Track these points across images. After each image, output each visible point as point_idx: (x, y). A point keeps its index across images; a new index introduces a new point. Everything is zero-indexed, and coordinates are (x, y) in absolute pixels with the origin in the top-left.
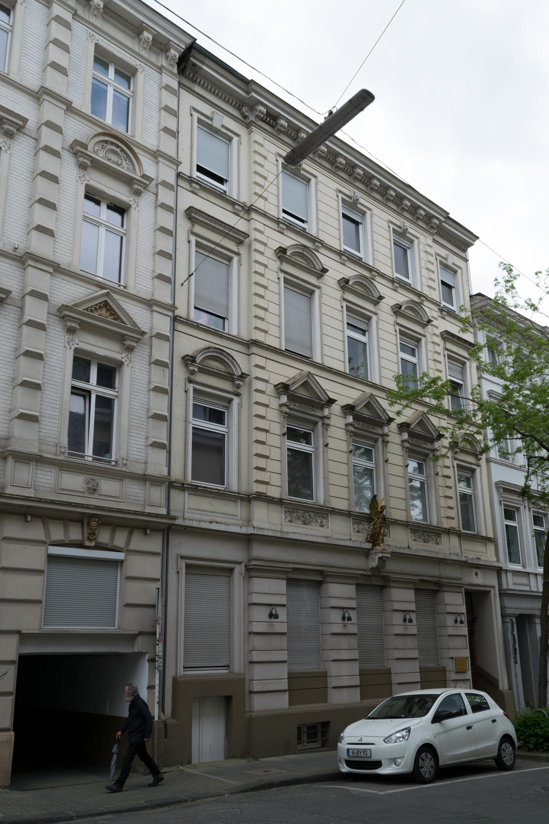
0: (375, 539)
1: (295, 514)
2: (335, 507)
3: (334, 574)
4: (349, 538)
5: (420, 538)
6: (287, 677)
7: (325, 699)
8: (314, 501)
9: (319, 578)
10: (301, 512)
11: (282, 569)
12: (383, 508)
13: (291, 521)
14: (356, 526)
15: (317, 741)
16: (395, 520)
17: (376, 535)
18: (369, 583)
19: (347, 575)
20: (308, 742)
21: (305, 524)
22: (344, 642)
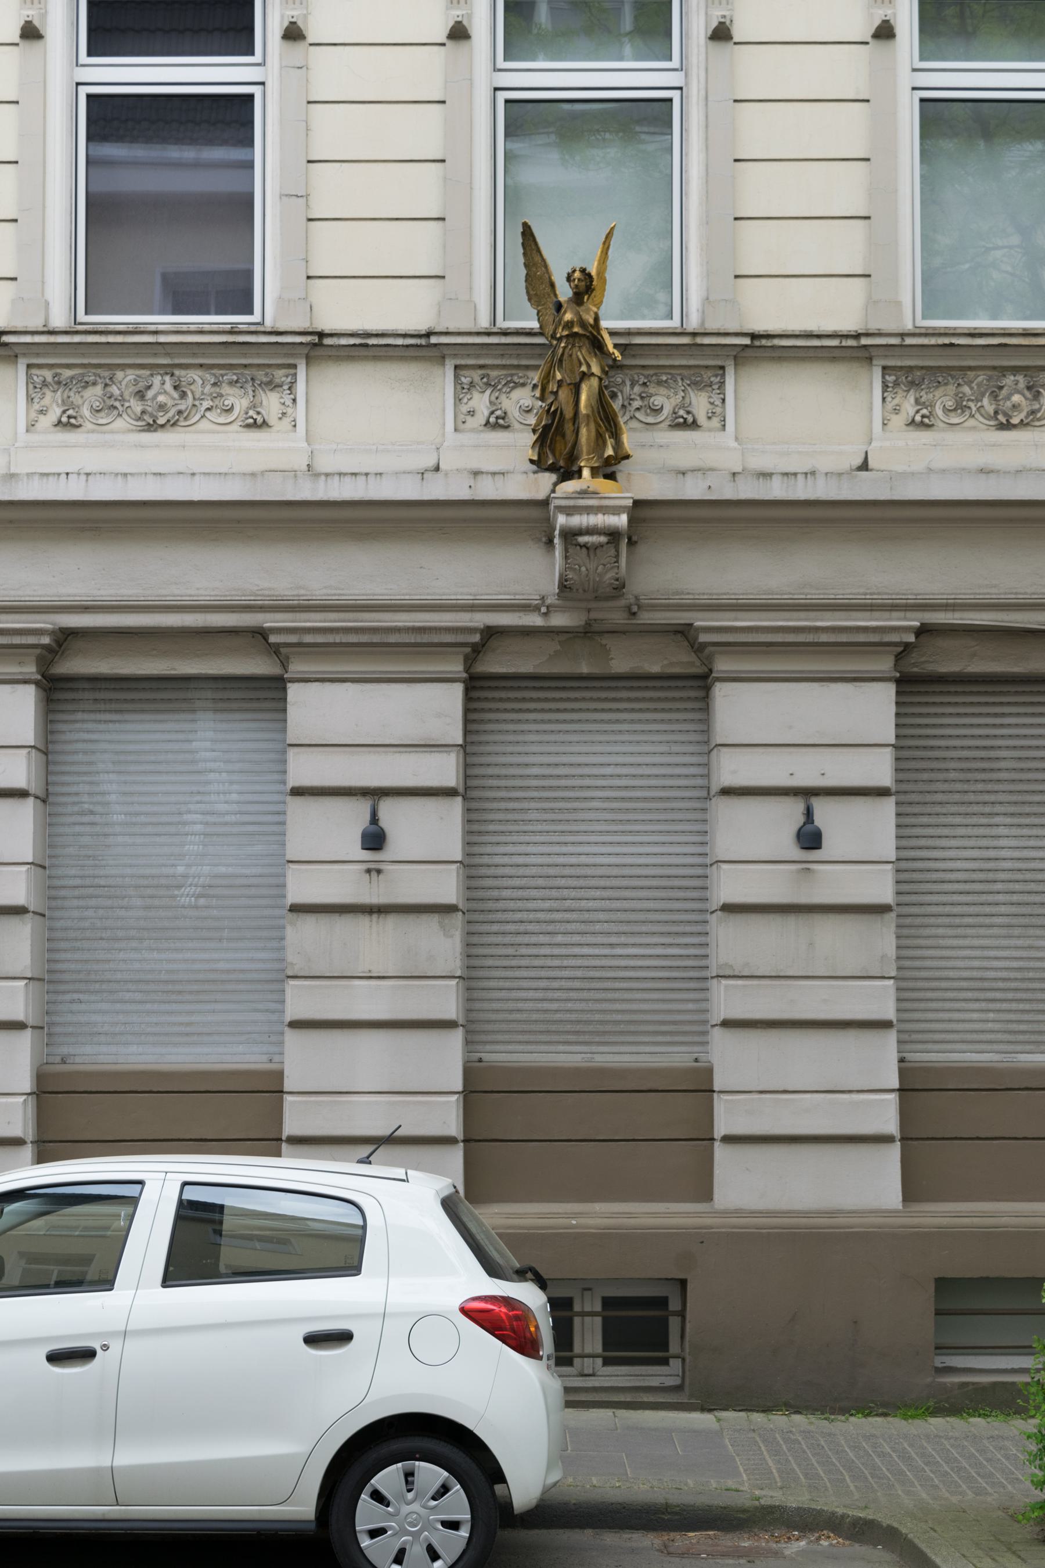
0: (556, 448)
1: (98, 390)
2: (326, 326)
3: (308, 639)
4: (431, 462)
5: (960, 407)
6: (895, 1084)
7: (702, 1188)
8: (256, 318)
9: (259, 666)
10: (131, 375)
11: (17, 640)
12: (586, 286)
13: (68, 424)
14: (481, 402)
15: (664, 1362)
16: (754, 336)
17: (569, 428)
18: (585, 669)
19: (392, 639)
20: (607, 1362)
21: (152, 427)
22: (375, 944)
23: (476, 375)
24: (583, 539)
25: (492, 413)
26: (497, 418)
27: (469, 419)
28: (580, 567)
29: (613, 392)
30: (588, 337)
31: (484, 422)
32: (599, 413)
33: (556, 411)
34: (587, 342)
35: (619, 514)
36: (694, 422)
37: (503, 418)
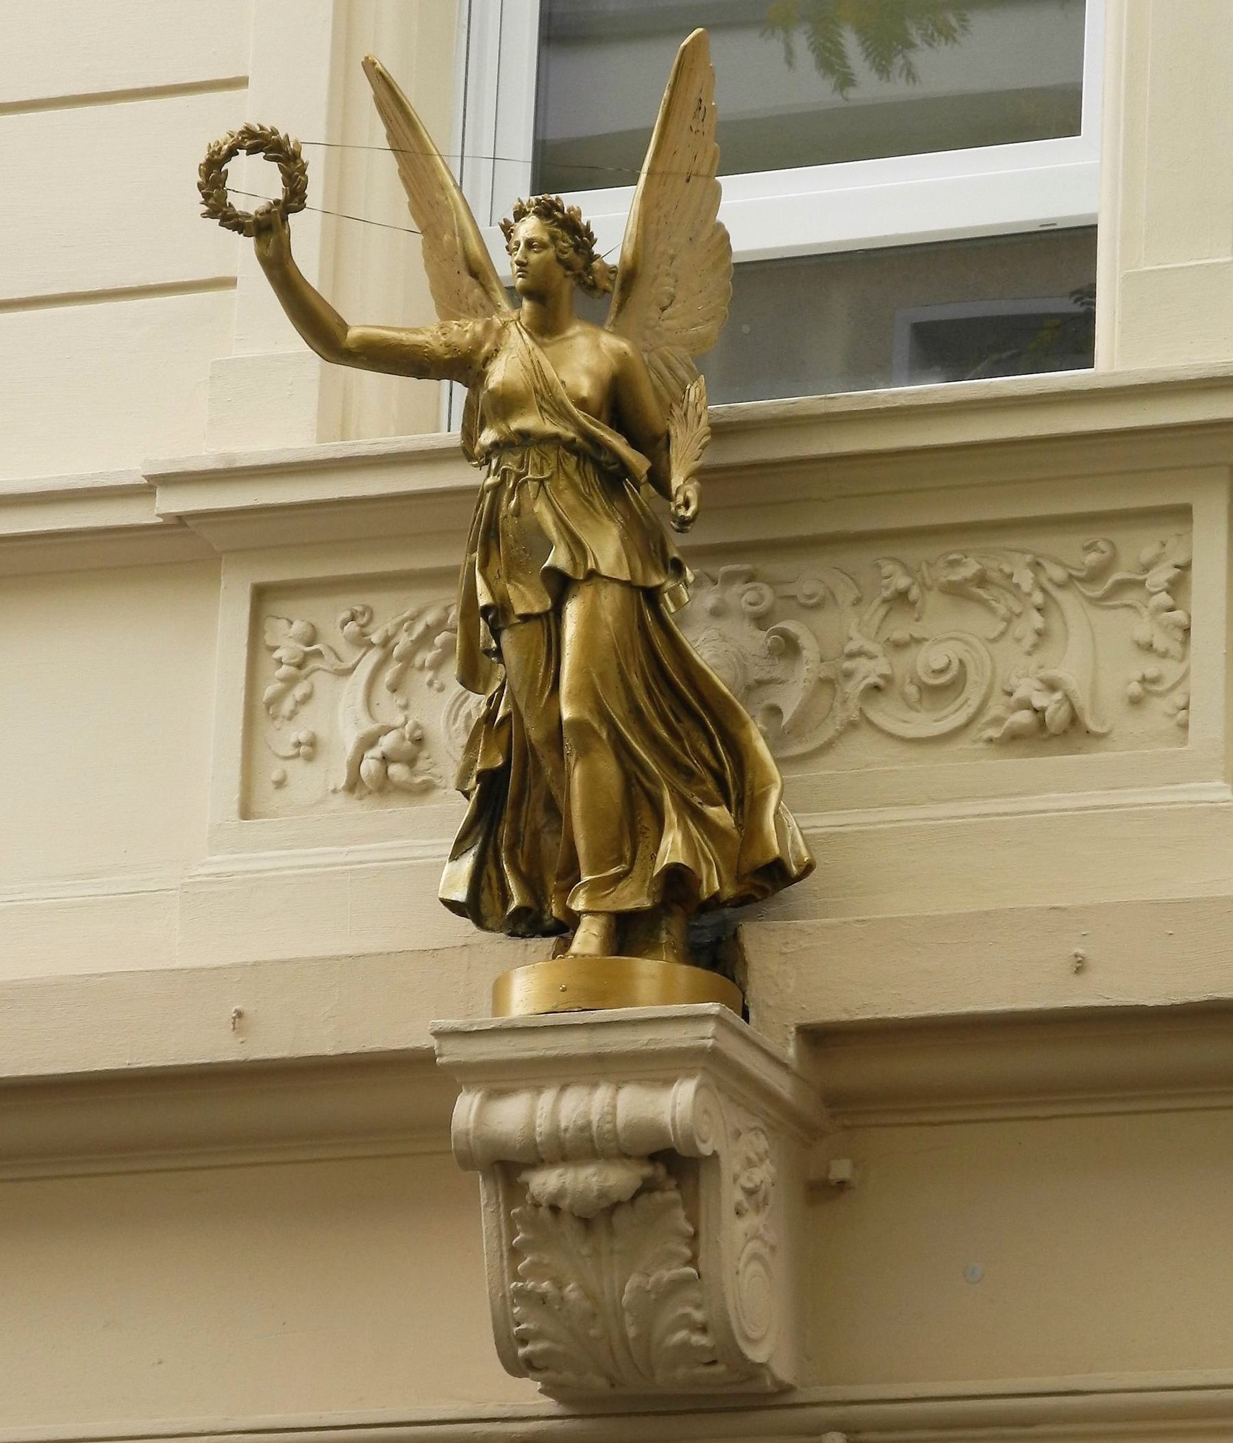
23: (331, 616)
24: (546, 1182)
25: (369, 741)
26: (385, 760)
27: (296, 769)
28: (559, 1284)
29: (784, 634)
30: (569, 445)
31: (342, 779)
32: (636, 713)
33: (507, 718)
34: (571, 463)
35: (668, 1083)
36: (1074, 720)
37: (411, 762)
